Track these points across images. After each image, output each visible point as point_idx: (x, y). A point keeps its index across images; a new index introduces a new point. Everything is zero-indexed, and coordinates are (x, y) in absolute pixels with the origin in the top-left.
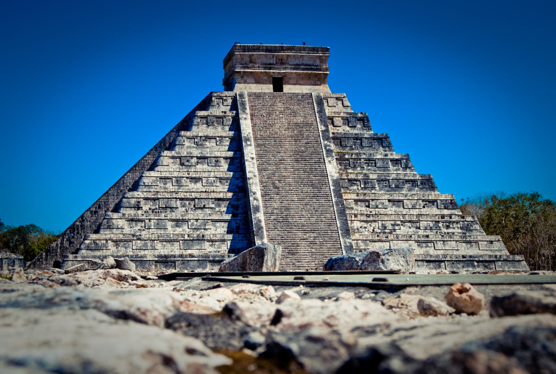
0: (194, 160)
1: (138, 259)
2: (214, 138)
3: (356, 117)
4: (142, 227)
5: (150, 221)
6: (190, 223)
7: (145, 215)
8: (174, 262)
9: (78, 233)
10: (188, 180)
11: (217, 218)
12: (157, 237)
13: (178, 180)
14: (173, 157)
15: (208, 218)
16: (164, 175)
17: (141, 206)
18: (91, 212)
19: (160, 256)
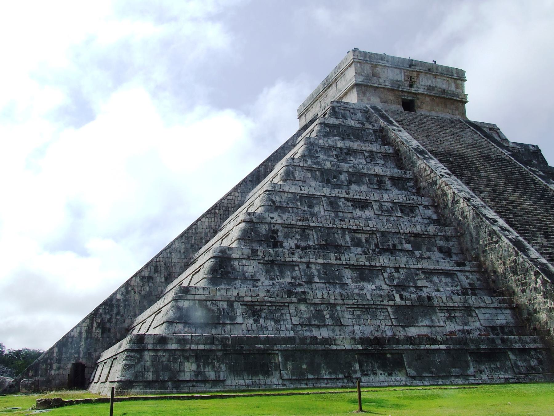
0: (344, 177)
1: (320, 348)
2: (362, 152)
3: (529, 150)
4: (293, 278)
5: (308, 267)
6: (385, 275)
7: (297, 255)
8: (400, 353)
9: (118, 313)
10: (349, 204)
11: (432, 267)
12: (338, 297)
13: (333, 203)
14: (309, 169)
15: (416, 266)
16: (305, 191)
17: (281, 239)
18: (143, 278)
19: (363, 341)
